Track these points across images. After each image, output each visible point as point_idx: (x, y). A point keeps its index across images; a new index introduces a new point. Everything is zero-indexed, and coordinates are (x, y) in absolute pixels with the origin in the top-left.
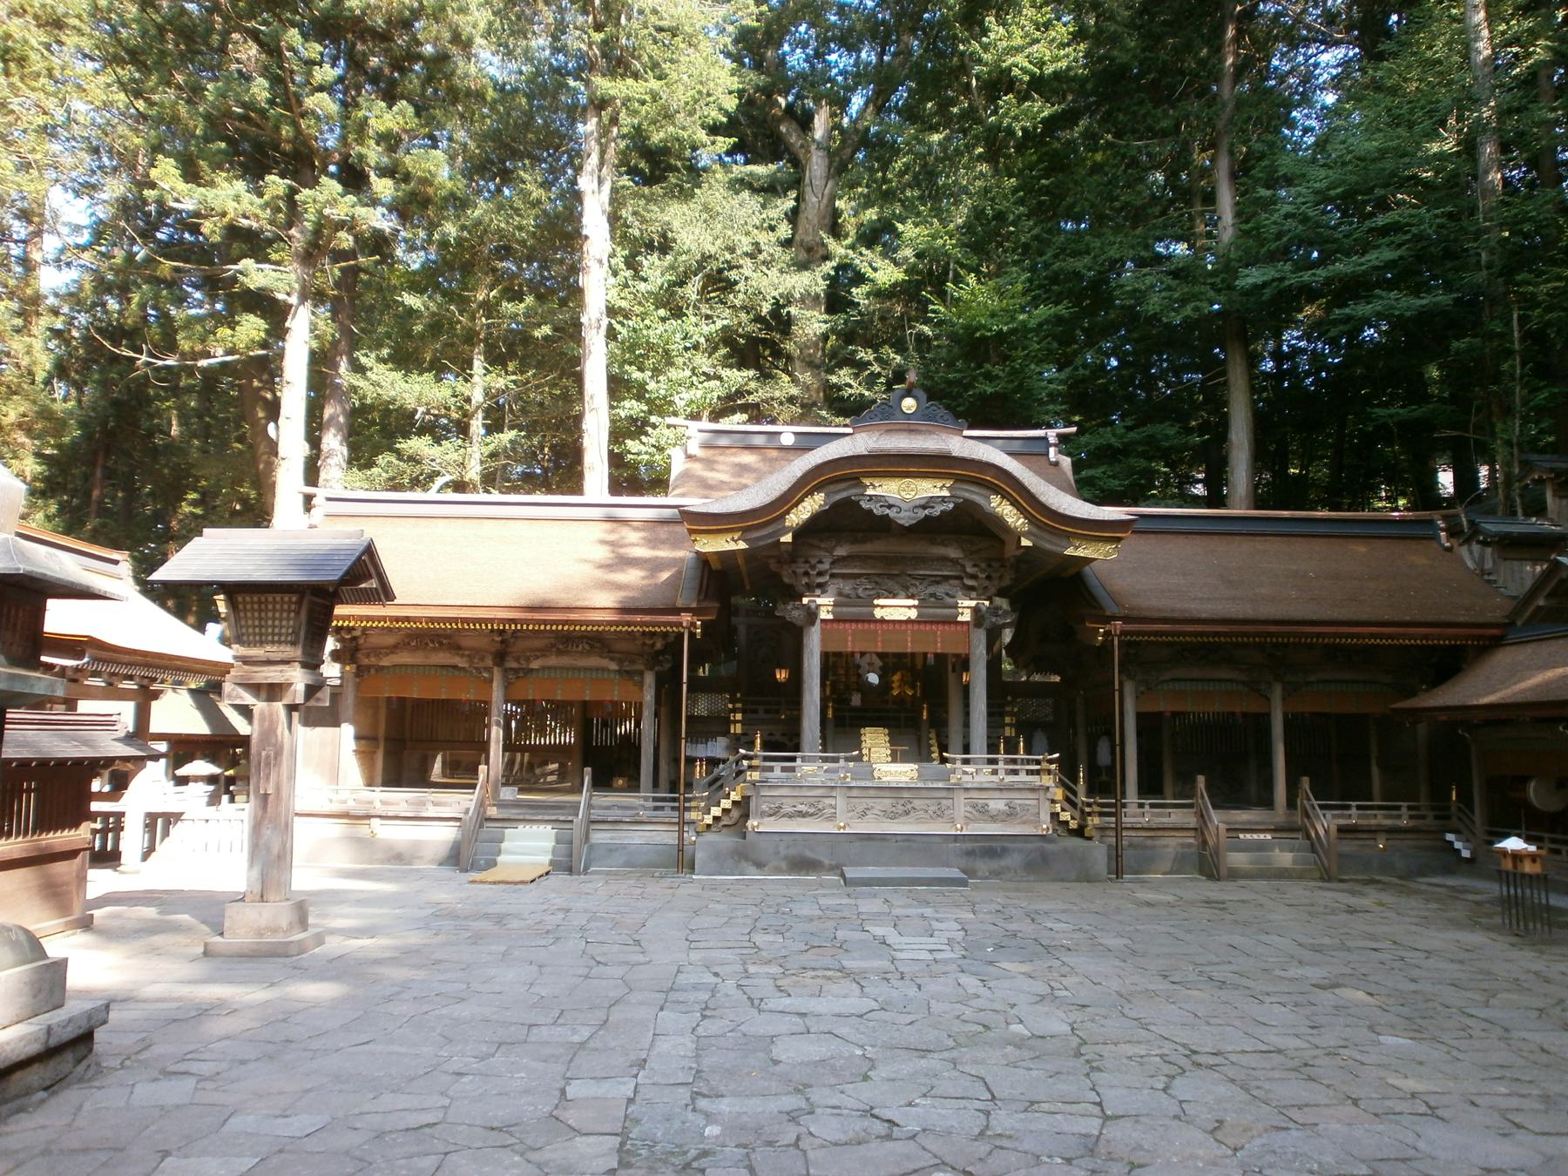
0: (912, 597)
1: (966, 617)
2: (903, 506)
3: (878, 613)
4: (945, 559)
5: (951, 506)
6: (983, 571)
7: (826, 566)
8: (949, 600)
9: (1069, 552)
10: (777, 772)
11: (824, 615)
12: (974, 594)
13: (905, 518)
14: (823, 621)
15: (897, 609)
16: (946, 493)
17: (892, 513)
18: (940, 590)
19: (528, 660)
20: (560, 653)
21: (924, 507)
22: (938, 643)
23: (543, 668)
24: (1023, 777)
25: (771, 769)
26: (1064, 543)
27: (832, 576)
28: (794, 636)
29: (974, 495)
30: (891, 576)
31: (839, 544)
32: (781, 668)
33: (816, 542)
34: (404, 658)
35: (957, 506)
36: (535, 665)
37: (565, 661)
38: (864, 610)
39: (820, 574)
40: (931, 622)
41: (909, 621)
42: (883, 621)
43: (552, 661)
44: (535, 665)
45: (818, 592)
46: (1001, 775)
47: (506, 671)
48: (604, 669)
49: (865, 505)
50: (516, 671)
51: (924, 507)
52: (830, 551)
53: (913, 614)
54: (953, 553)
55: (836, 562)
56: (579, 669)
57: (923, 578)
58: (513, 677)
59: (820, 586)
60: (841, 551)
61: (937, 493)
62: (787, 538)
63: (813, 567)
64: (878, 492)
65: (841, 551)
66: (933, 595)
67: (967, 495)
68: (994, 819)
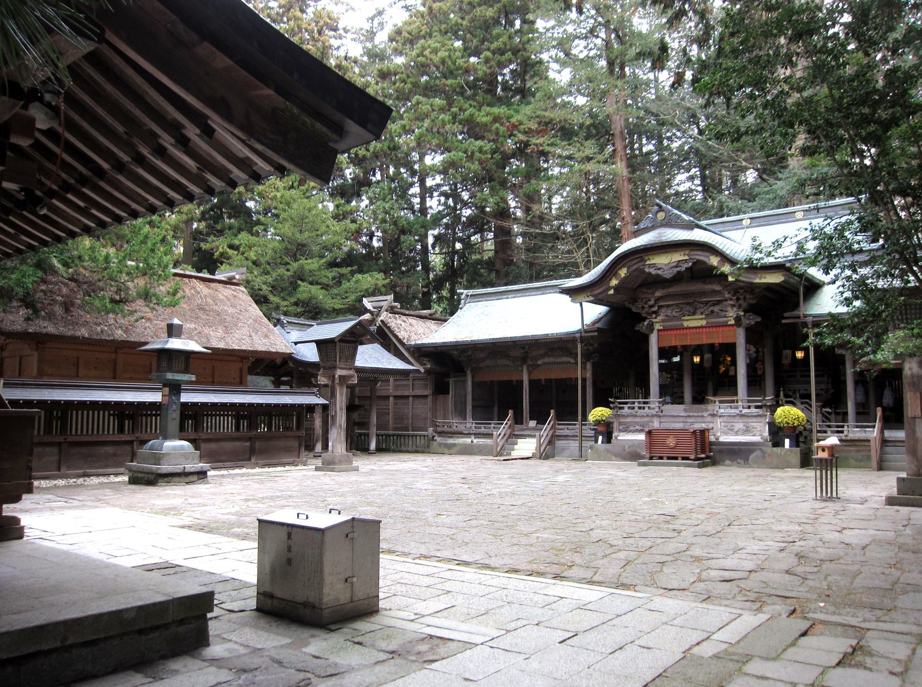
0: (702, 314)
1: (733, 322)
2: (666, 268)
3: (686, 324)
4: (714, 292)
5: (690, 264)
6: (734, 295)
7: (652, 302)
8: (723, 313)
9: (757, 281)
10: (626, 409)
11: (657, 327)
12: (735, 309)
13: (668, 274)
14: (659, 330)
15: (695, 321)
16: (687, 258)
17: (660, 272)
18: (716, 309)
19: (536, 360)
20: (549, 356)
21: (677, 267)
22: (718, 338)
23: (545, 364)
24: (753, 410)
25: (623, 408)
26: (753, 276)
27: (660, 307)
28: (645, 339)
29: (700, 256)
30: (688, 304)
31: (656, 290)
32: (696, 356)
33: (645, 290)
34: (488, 362)
35: (694, 264)
36: (539, 362)
37: (552, 359)
38: (679, 323)
39: (652, 306)
40: (716, 326)
41: (702, 327)
42: (690, 328)
43: (546, 360)
44: (539, 362)
45: (654, 316)
46: (741, 409)
47: (528, 366)
48: (569, 362)
49: (647, 270)
50: (532, 366)
51: (677, 267)
52: (653, 293)
53: (704, 323)
54: (717, 288)
55: (658, 299)
56: (557, 363)
57: (707, 303)
58: (533, 368)
59: (654, 312)
60: (658, 294)
61: (682, 258)
62: (612, 292)
63: (646, 303)
64: (652, 262)
65: (658, 294)
66: (712, 312)
67: (697, 257)
68: (737, 433)
